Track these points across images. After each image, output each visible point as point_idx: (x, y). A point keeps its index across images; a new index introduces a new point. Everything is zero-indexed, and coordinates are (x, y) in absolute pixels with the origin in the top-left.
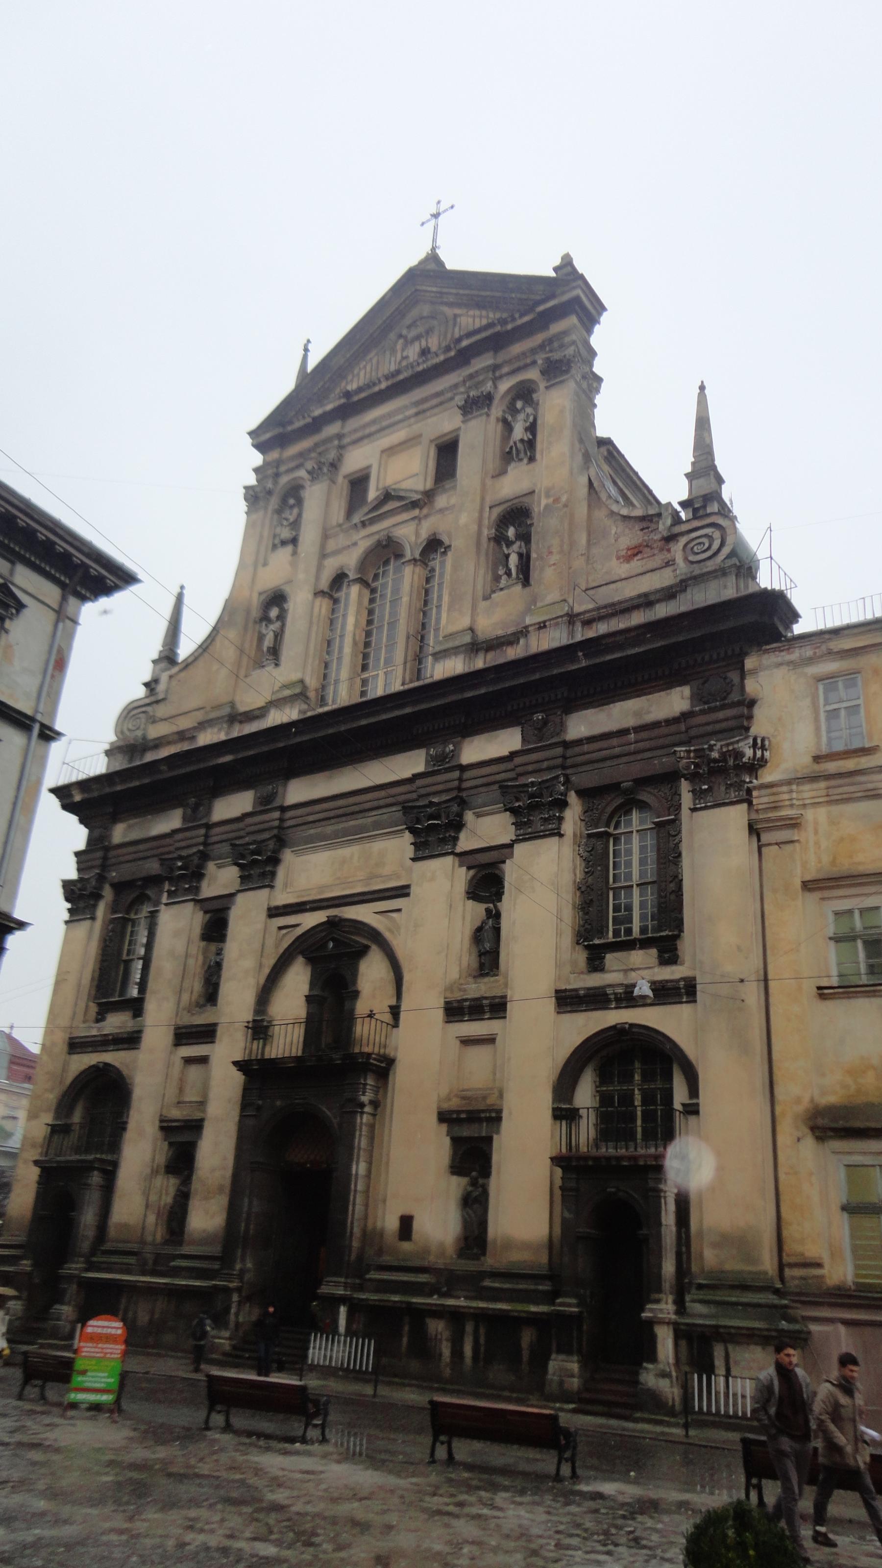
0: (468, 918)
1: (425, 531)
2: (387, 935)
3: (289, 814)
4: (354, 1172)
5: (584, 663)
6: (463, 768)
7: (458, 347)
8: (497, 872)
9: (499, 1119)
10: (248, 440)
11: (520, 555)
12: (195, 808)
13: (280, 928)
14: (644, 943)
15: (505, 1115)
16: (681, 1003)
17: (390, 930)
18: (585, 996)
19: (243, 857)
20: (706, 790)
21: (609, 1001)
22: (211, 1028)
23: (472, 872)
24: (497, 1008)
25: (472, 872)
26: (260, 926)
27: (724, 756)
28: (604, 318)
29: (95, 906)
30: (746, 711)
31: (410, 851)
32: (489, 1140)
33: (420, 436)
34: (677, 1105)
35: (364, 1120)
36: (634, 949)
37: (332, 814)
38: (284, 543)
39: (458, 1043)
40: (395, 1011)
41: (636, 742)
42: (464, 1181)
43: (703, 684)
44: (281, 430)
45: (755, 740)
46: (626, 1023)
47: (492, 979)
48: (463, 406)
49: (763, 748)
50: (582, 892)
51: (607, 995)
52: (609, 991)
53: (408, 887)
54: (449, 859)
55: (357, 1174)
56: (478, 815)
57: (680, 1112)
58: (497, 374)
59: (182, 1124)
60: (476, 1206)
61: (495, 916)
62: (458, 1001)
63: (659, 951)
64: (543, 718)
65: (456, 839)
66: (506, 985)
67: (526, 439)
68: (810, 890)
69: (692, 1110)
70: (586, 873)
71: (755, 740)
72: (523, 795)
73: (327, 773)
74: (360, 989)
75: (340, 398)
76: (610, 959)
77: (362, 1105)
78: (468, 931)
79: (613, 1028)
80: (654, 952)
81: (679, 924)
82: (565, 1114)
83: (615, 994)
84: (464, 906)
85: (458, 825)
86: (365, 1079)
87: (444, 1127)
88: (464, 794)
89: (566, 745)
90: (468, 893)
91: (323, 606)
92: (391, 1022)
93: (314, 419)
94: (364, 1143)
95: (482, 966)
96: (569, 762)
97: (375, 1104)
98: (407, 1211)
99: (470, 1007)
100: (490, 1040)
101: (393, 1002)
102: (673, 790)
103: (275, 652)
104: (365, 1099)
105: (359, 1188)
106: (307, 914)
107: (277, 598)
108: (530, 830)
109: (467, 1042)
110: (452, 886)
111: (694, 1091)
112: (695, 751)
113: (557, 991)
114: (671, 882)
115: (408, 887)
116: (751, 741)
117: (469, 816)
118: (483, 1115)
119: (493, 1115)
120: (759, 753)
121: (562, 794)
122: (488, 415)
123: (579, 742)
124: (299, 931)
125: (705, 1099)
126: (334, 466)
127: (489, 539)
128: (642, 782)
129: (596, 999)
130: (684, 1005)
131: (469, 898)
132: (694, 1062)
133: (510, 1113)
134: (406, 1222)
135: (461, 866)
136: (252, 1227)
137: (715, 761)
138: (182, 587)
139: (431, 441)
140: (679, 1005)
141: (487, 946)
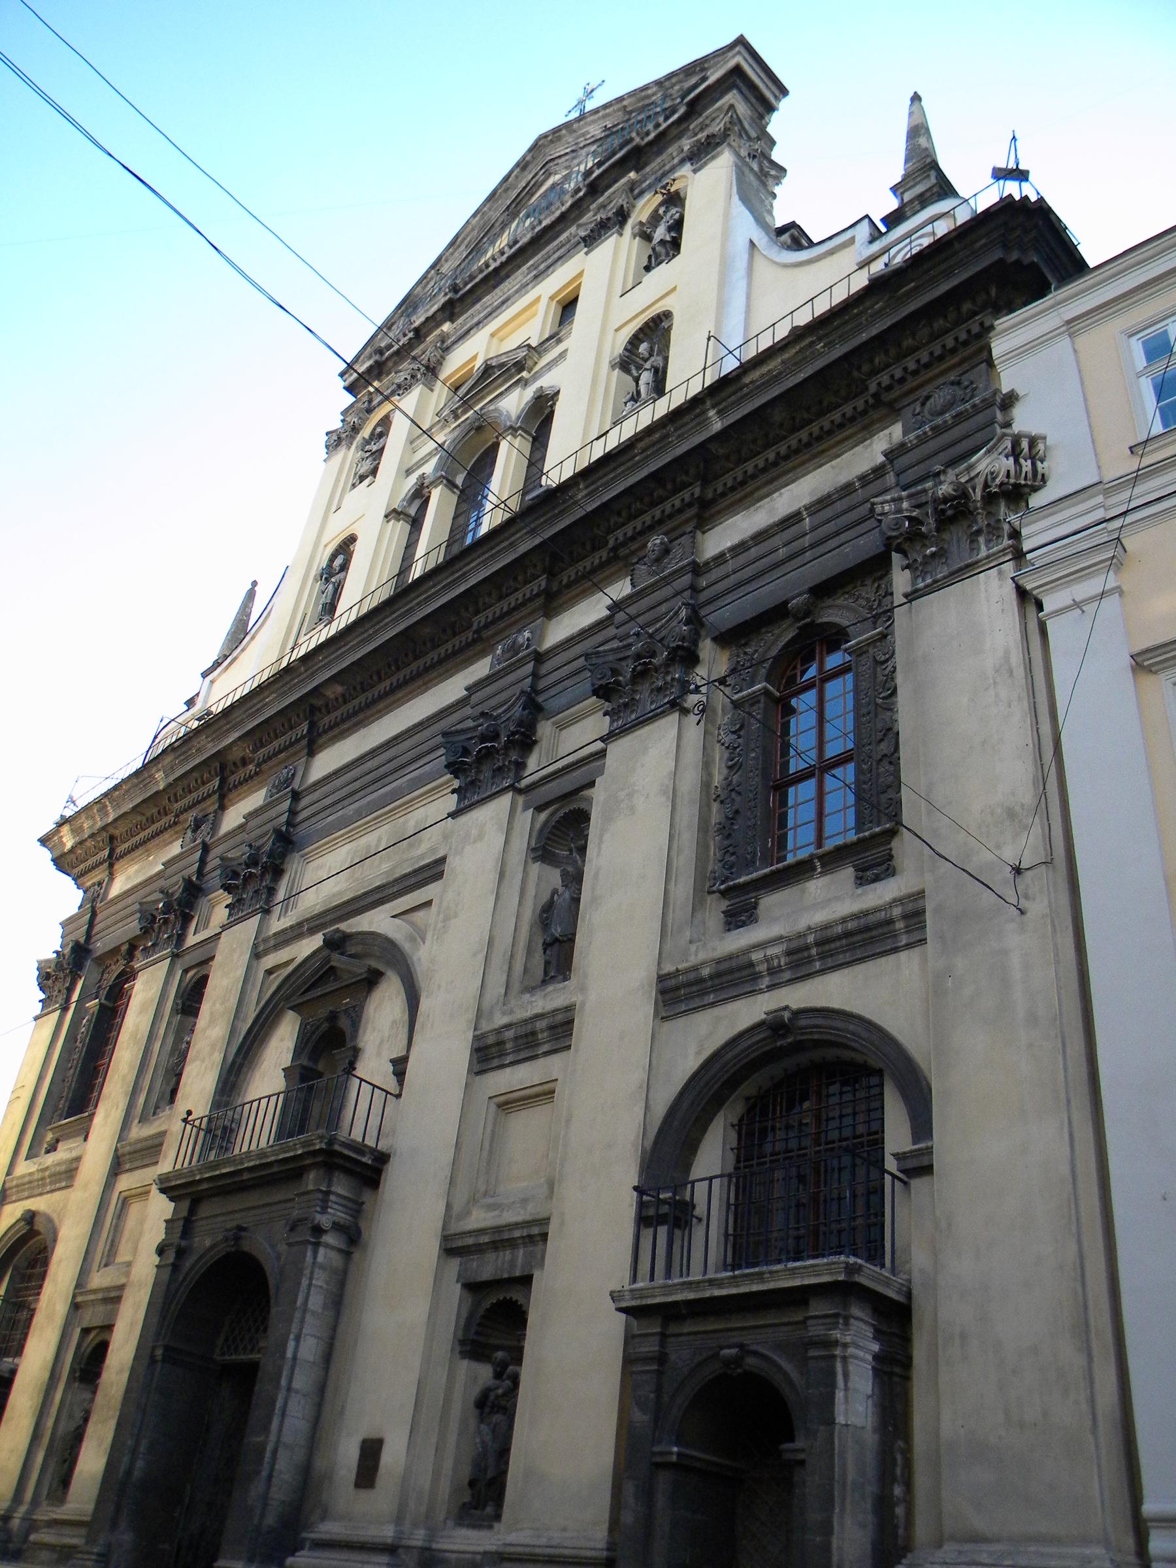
0: (531, 892)
1: (529, 393)
2: (406, 947)
3: (304, 802)
4: (289, 1354)
5: (717, 426)
6: (539, 658)
7: (587, 182)
8: (583, 806)
9: (544, 1237)
10: (341, 383)
11: (656, 370)
12: (197, 825)
13: (269, 972)
14: (832, 860)
15: (552, 1230)
16: (895, 950)
17: (412, 939)
18: (711, 977)
19: (235, 875)
20: (933, 555)
21: (756, 977)
22: (156, 1141)
23: (543, 816)
24: (559, 1031)
25: (543, 816)
26: (240, 972)
27: (962, 494)
28: (784, 105)
29: (70, 990)
30: (999, 416)
31: (450, 802)
32: (526, 1281)
33: (538, 299)
34: (891, 1164)
35: (320, 1258)
36: (811, 878)
37: (357, 784)
38: (362, 478)
39: (493, 1108)
40: (400, 1067)
41: (813, 529)
42: (485, 1373)
43: (923, 404)
44: (377, 357)
45: (1016, 443)
46: (786, 1008)
47: (561, 985)
48: (589, 236)
49: (1033, 458)
50: (722, 802)
51: (751, 965)
52: (756, 956)
53: (442, 860)
54: (506, 800)
55: (295, 1358)
56: (561, 727)
57: (894, 1176)
58: (636, 192)
59: (100, 1296)
60: (497, 1418)
61: (574, 879)
62: (498, 1031)
63: (858, 869)
64: (661, 543)
65: (521, 766)
67: (668, 238)
68: (1149, 670)
69: (919, 1167)
70: (730, 768)
71: (1016, 443)
72: (624, 663)
73: (362, 732)
74: (361, 1045)
75: (446, 294)
76: (770, 902)
77: (318, 1230)
78: (528, 914)
79: (760, 1025)
80: (847, 873)
81: (894, 812)
82: (662, 1207)
83: (767, 960)
84: (525, 871)
85: (526, 742)
86: (329, 1186)
87: (454, 1264)
88: (540, 699)
89: (697, 569)
91: (400, 529)
92: (391, 1084)
93: (417, 331)
94: (316, 1302)
95: (547, 963)
96: (703, 597)
97: (353, 1237)
98: (374, 1435)
99: (516, 1038)
100: (544, 1094)
101: (404, 1053)
102: (882, 592)
103: (330, 609)
104: (325, 1221)
105: (297, 1384)
106: (304, 942)
107: (346, 547)
108: (633, 717)
109: (508, 1104)
110: (506, 842)
111: (922, 1125)
112: (910, 496)
113: (661, 979)
114: (882, 740)
115: (442, 860)
116: (1008, 443)
118: (517, 1234)
119: (535, 1231)
120: (1027, 466)
121: (683, 639)
122: (621, 235)
123: (720, 559)
124: (290, 968)
125: (942, 1138)
126: (432, 371)
127: (613, 367)
128: (824, 590)
129: (734, 978)
130: (903, 956)
131: (535, 859)
132: (923, 1065)
133: (562, 1223)
134: (371, 1450)
136: (140, 1464)
137: (945, 500)
138: (255, 583)
139: (552, 298)
140: (891, 958)
141: (557, 931)
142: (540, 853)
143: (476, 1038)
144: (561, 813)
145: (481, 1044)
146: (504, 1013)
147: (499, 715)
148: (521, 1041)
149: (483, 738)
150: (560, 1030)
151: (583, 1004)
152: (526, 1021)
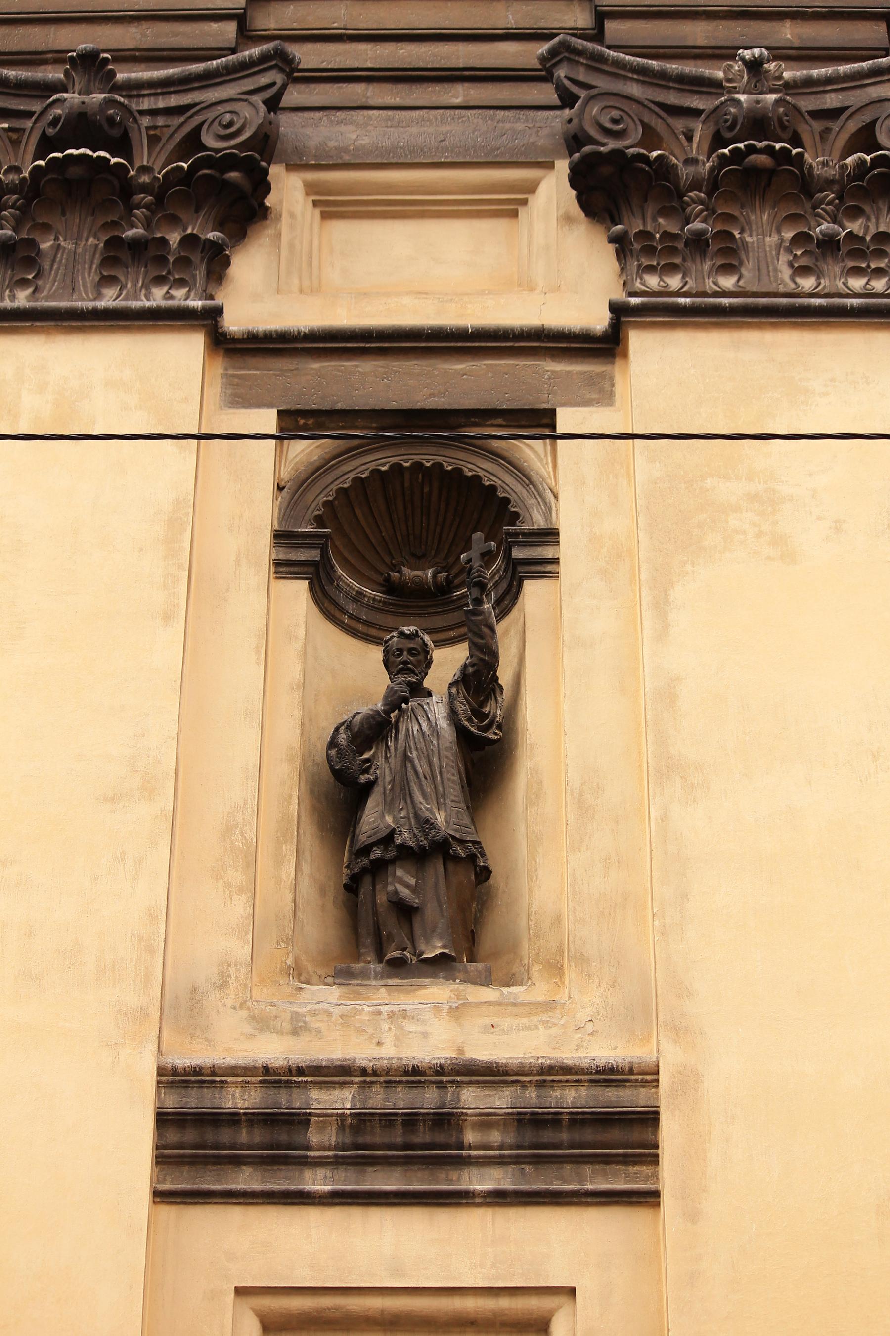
56: (331, 207)
62: (271, 1077)
65: (217, 263)
66: (641, 1014)
72: (679, 124)
85: (243, 208)
90: (281, 537)
99: (360, 1121)
117: (288, 190)
131: (284, 569)
135: (240, 397)
142: (314, 555)
143: (171, 1078)
144: (382, 461)
145: (194, 1100)
146: (263, 1024)
147: (133, 88)
148: (378, 1136)
149: (81, 127)
150: (564, 1136)
151: (690, 1079)
152: (414, 1075)
